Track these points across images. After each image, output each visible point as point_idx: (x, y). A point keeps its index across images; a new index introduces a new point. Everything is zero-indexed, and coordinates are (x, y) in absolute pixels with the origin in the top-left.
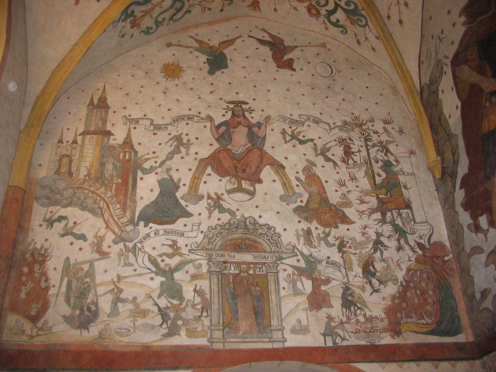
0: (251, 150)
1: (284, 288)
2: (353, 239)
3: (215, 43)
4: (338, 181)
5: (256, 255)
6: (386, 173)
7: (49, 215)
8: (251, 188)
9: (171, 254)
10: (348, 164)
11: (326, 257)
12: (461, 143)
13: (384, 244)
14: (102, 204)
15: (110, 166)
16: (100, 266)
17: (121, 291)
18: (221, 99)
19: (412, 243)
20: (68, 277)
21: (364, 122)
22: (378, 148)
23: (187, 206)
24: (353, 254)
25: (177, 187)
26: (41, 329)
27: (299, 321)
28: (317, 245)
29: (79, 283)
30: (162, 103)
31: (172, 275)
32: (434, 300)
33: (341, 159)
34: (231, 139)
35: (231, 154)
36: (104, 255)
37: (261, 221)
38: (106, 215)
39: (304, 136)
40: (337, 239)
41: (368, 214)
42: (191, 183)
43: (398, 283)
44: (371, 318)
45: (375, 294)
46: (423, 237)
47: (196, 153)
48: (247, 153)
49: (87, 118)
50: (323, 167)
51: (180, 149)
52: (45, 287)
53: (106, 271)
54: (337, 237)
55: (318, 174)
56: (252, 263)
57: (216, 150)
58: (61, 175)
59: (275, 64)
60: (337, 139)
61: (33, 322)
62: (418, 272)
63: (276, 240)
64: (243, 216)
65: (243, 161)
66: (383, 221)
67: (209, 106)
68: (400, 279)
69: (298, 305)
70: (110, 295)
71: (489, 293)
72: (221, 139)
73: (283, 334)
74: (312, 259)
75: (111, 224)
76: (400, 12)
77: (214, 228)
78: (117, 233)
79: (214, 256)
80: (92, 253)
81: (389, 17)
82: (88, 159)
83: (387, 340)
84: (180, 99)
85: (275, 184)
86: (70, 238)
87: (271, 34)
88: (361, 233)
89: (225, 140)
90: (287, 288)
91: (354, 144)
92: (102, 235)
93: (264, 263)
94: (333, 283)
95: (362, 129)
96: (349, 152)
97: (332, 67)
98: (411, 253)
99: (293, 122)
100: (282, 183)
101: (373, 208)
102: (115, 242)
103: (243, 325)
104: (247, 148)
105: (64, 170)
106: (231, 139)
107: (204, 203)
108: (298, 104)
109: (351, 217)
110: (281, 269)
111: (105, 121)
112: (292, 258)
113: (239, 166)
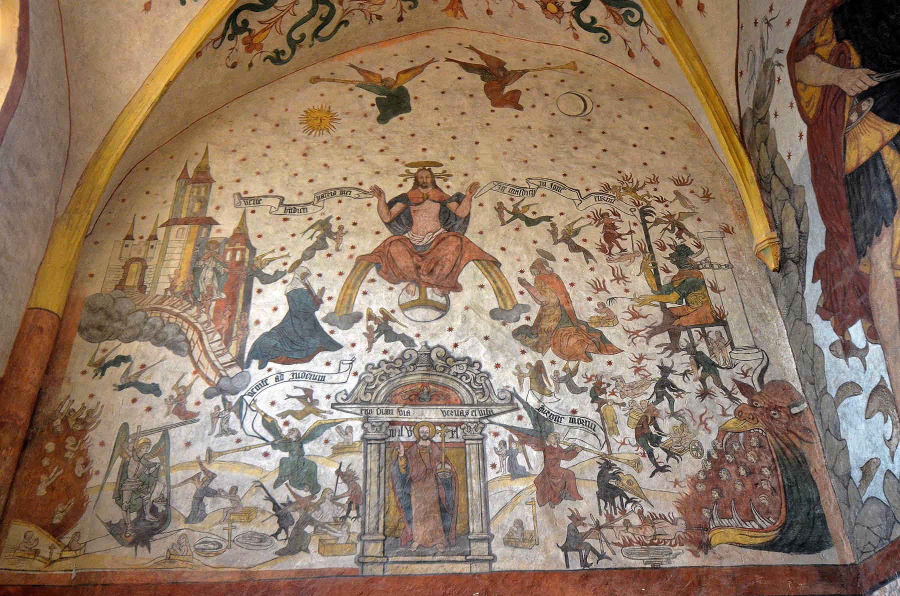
0: (444, 239)
1: (494, 466)
2: (619, 379)
3: (391, 74)
4: (592, 283)
5: (446, 410)
6: (679, 267)
7: (100, 355)
8: (442, 300)
9: (301, 411)
10: (610, 254)
11: (570, 410)
12: (811, 199)
13: (674, 386)
15: (208, 274)
17: (212, 477)
18: (397, 160)
19: (729, 385)
20: (122, 457)
21: (641, 184)
22: (665, 226)
23: (332, 332)
24: (617, 404)
27: (519, 523)
28: (553, 390)
29: (141, 465)
30: (300, 170)
31: (301, 447)
32: (773, 485)
33: (598, 247)
34: (412, 223)
36: (188, 418)
37: (458, 353)
38: (197, 353)
39: (534, 213)
40: (589, 380)
41: (646, 335)
42: (342, 295)
43: (702, 454)
44: (653, 519)
45: (660, 476)
46: (750, 373)
47: (353, 247)
48: (438, 244)
49: (176, 200)
50: (567, 260)
51: (326, 242)
52: (83, 474)
53: (188, 444)
54: (589, 377)
55: (559, 272)
56: (440, 424)
57: (386, 240)
58: (126, 290)
59: (488, 102)
60: (592, 215)
61: (55, 536)
62: (741, 435)
63: (481, 384)
64: (426, 345)
65: (430, 257)
66: (674, 347)
67: (378, 173)
68: (707, 447)
70: (193, 485)
71: (877, 467)
72: (395, 223)
73: (489, 548)
74: (545, 415)
75: (203, 365)
77: (376, 366)
78: (213, 379)
80: (168, 414)
82: (175, 263)
84: (330, 163)
85: (483, 291)
86: (132, 391)
87: (484, 54)
88: (633, 369)
89: (401, 223)
90: (498, 466)
91: (621, 221)
92: (187, 384)
93: (460, 424)
94: (583, 456)
95: (637, 197)
96: (613, 235)
97: (586, 99)
98: (726, 402)
99: (517, 190)
100: (495, 288)
101: (656, 325)
102: (208, 395)
103: (419, 532)
104: (437, 236)
105: (132, 282)
106: (410, 223)
107: (361, 327)
108: (526, 162)
109: (616, 342)
110: (490, 433)
111: (204, 203)
112: (509, 414)
113: (423, 264)
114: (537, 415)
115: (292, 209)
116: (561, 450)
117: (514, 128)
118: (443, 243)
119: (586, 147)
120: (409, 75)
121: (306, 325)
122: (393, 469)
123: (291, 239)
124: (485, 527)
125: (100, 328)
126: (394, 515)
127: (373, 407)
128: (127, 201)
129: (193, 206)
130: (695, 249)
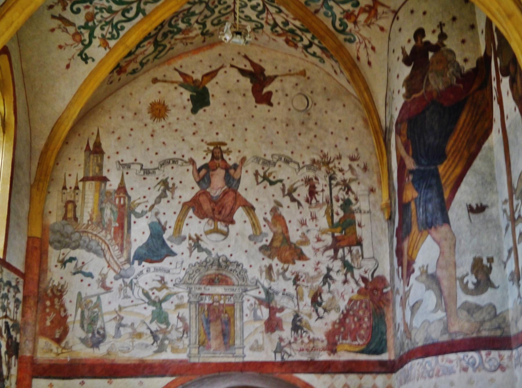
1: (247, 315)
2: (307, 274)
3: (198, 76)
6: (345, 211)
7: (61, 257)
8: (225, 229)
10: (311, 203)
14: (103, 246)
15: (108, 212)
16: (105, 298)
17: (122, 318)
19: (357, 277)
21: (332, 160)
23: (172, 246)
25: (164, 229)
26: (64, 348)
27: (257, 341)
30: (150, 146)
35: (209, 197)
36: (108, 289)
37: (232, 259)
38: (108, 256)
40: (293, 274)
42: (176, 225)
43: (339, 311)
45: (319, 321)
46: (368, 272)
53: (110, 303)
55: (284, 214)
56: (223, 295)
58: (68, 220)
59: (253, 100)
60: (304, 180)
64: (217, 254)
65: (220, 203)
66: (335, 257)
67: (192, 149)
69: (256, 329)
72: (201, 182)
76: (368, 54)
79: (193, 289)
80: (98, 287)
81: (358, 58)
83: (324, 357)
85: (246, 224)
86: (79, 276)
90: (249, 316)
94: (286, 311)
95: (329, 168)
99: (266, 163)
102: (116, 279)
103: (214, 344)
105: (70, 215)
106: (210, 182)
107: (186, 244)
111: (101, 167)
114: (268, 292)
115: (147, 172)
116: (277, 309)
117: (267, 119)
118: (226, 195)
119: (305, 134)
120: (209, 77)
121: (159, 242)
122: (203, 316)
123: (148, 191)
124: (242, 342)
125: (59, 242)
126: (203, 337)
127: (193, 286)
128: (60, 165)
129: (95, 169)
130: (354, 201)
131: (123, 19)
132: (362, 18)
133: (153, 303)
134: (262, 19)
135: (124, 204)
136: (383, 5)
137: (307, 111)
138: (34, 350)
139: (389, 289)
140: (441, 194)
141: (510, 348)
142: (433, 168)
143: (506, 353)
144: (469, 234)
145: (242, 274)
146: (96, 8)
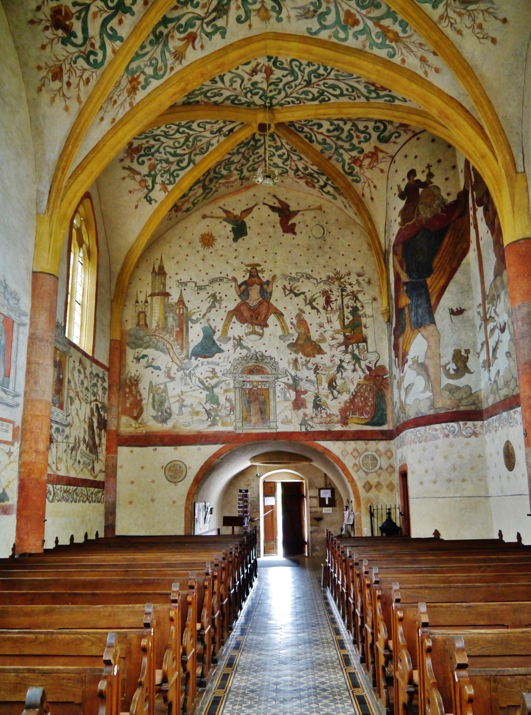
2: (324, 365)
3: (237, 212)
7: (136, 355)
8: (261, 331)
14: (168, 346)
15: (170, 319)
16: (170, 385)
17: (184, 400)
19: (363, 367)
25: (214, 332)
26: (140, 424)
27: (286, 417)
30: (202, 268)
36: (172, 379)
37: (267, 354)
38: (171, 353)
45: (334, 400)
49: (152, 283)
55: (306, 319)
59: (281, 230)
65: (256, 312)
66: (346, 352)
81: (363, 195)
83: (338, 428)
86: (150, 369)
94: (309, 393)
99: (292, 279)
102: (178, 371)
103: (254, 419)
105: (142, 322)
107: (231, 343)
111: (164, 285)
113: (253, 315)
114: (295, 379)
115: (200, 288)
120: (246, 213)
122: (245, 398)
125: (134, 343)
126: (245, 414)
127: (237, 375)
130: (360, 308)
131: (178, 168)
132: (366, 162)
133: (207, 389)
134: (287, 165)
135: (183, 314)
136: (383, 152)
137: (323, 238)
138: (118, 426)
139: (388, 375)
140: (428, 301)
141: (483, 420)
142: (422, 280)
143: (479, 423)
144: (450, 331)
145: (275, 366)
146: (157, 160)
